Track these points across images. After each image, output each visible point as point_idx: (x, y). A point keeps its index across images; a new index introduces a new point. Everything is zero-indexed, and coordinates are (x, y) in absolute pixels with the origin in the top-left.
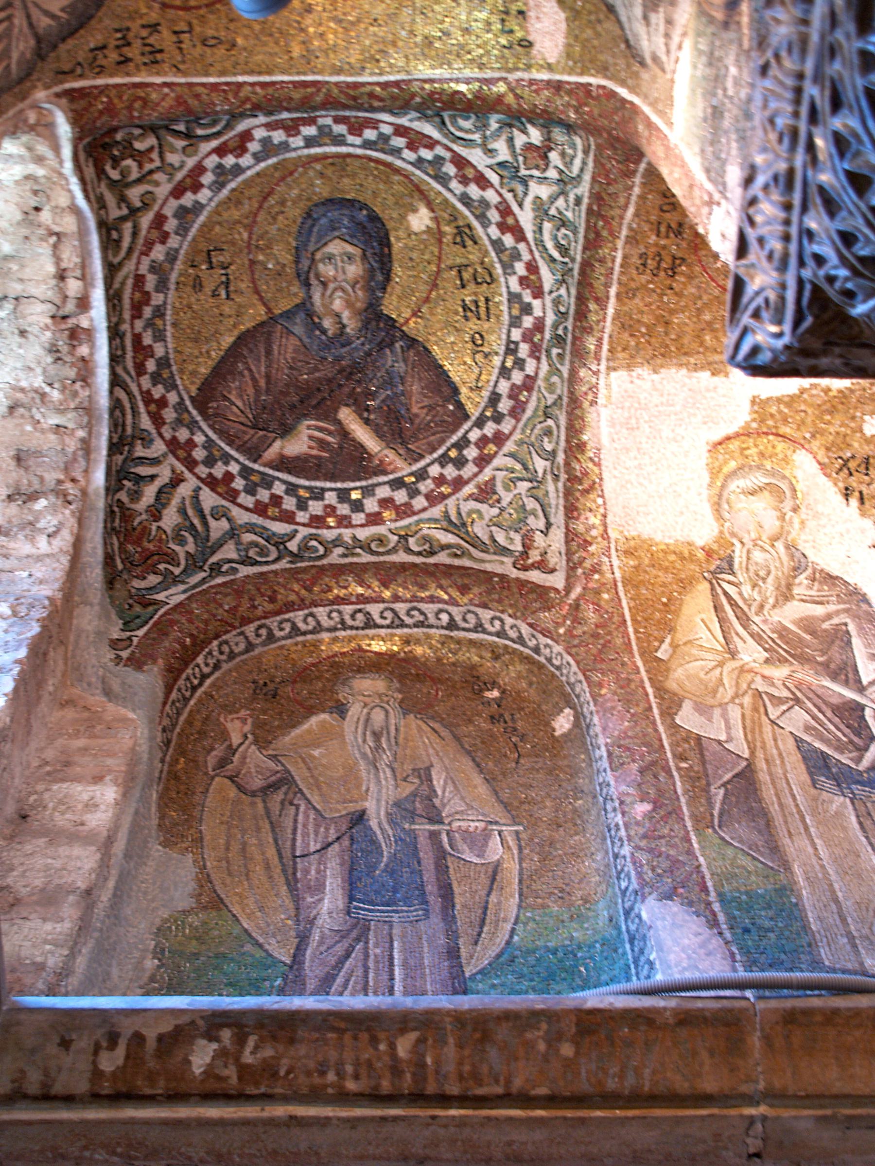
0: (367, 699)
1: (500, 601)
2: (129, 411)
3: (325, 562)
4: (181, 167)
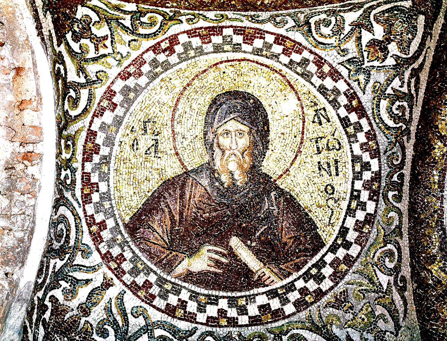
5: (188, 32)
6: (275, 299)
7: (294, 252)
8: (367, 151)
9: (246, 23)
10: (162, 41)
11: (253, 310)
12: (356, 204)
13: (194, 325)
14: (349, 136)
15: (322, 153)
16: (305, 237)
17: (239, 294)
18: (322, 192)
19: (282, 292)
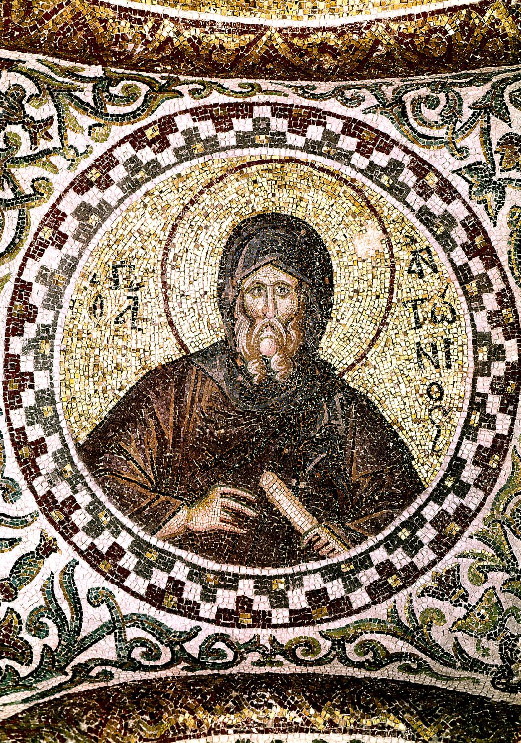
3: (234, 670)
4: (86, 153)
5: (193, 112)
6: (335, 581)
7: (372, 501)
8: (499, 325)
9: (294, 99)
10: (146, 127)
11: (297, 599)
12: (478, 418)
14: (469, 299)
15: (425, 327)
16: (391, 474)
17: (274, 572)
18: (422, 396)
19: (348, 569)
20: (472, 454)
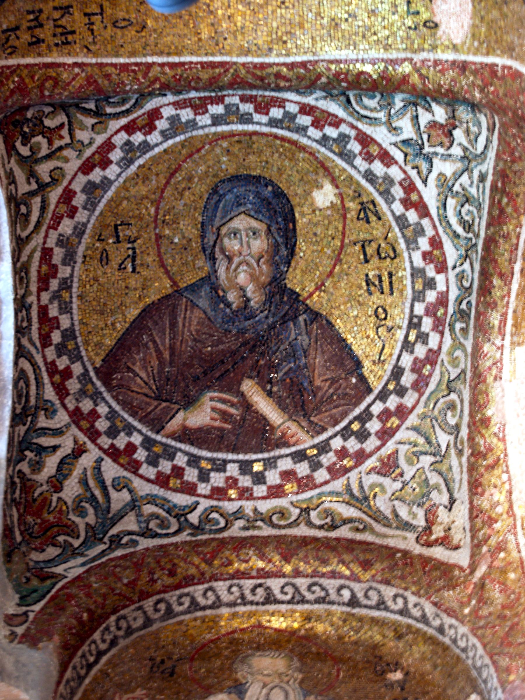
0: (267, 679)
1: (403, 578)
2: (33, 382)
3: (226, 534)
4: (90, 143)
13: (194, 499)
14: (408, 242)
17: (254, 457)
20: (410, 364)
